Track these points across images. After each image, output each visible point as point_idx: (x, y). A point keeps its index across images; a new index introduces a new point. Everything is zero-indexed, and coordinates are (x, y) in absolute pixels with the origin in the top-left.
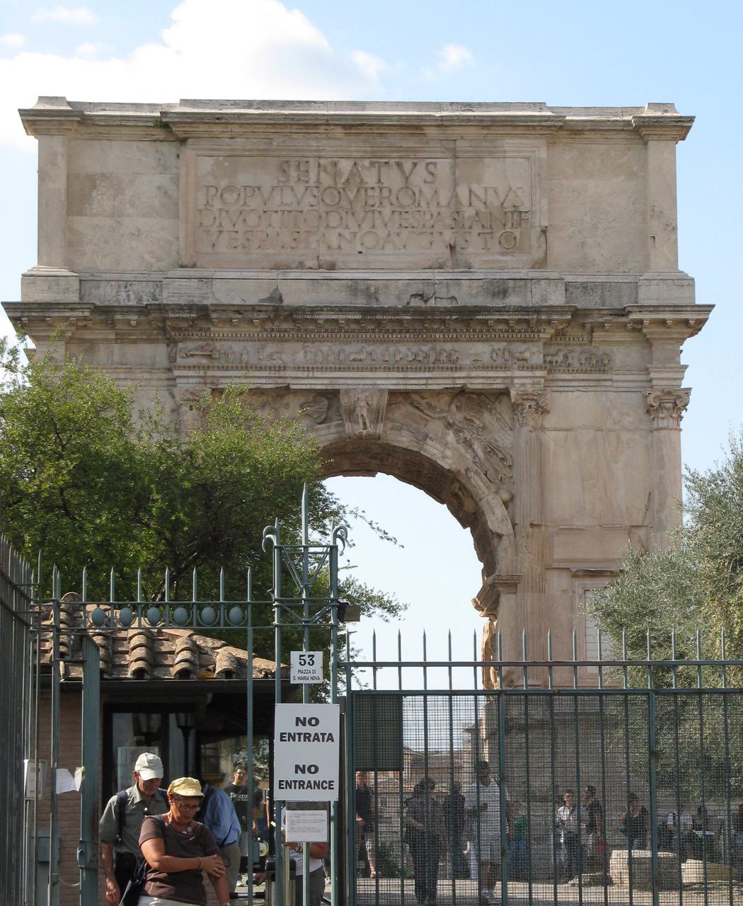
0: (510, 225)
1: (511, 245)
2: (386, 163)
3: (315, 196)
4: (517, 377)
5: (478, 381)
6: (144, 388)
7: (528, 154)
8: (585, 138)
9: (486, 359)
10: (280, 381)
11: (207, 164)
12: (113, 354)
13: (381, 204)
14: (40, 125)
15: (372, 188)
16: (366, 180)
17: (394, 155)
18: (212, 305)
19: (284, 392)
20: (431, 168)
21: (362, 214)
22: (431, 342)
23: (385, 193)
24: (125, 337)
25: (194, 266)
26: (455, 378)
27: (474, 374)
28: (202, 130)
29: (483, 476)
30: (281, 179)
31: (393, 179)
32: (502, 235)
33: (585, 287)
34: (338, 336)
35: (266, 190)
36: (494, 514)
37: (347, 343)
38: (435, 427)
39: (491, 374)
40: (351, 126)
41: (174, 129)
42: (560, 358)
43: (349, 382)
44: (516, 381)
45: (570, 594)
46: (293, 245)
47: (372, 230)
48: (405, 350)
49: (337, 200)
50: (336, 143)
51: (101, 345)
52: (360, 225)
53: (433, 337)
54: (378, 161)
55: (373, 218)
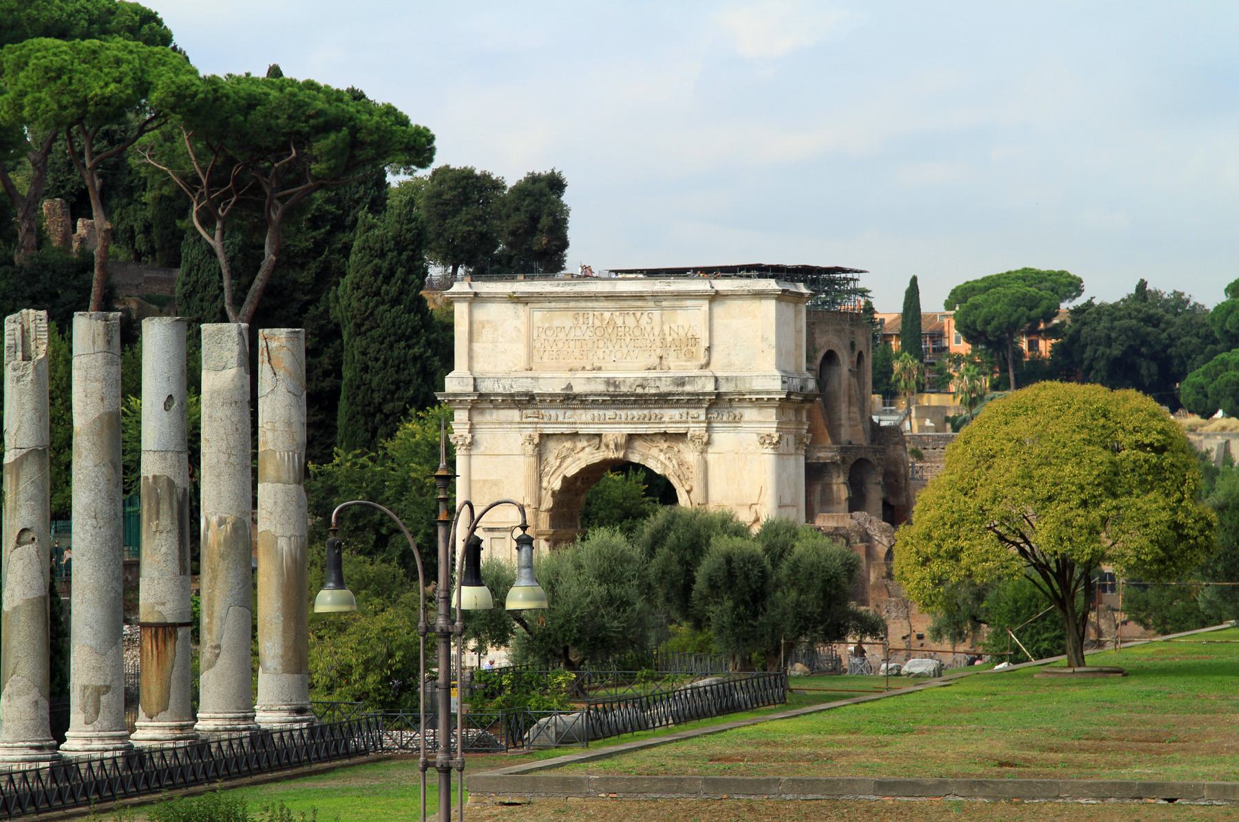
1: (691, 356)
9: (677, 418)
19: (575, 435)
23: (627, 329)
31: (630, 321)
35: (567, 329)
37: (606, 409)
38: (654, 451)
39: (678, 425)
48: (636, 413)
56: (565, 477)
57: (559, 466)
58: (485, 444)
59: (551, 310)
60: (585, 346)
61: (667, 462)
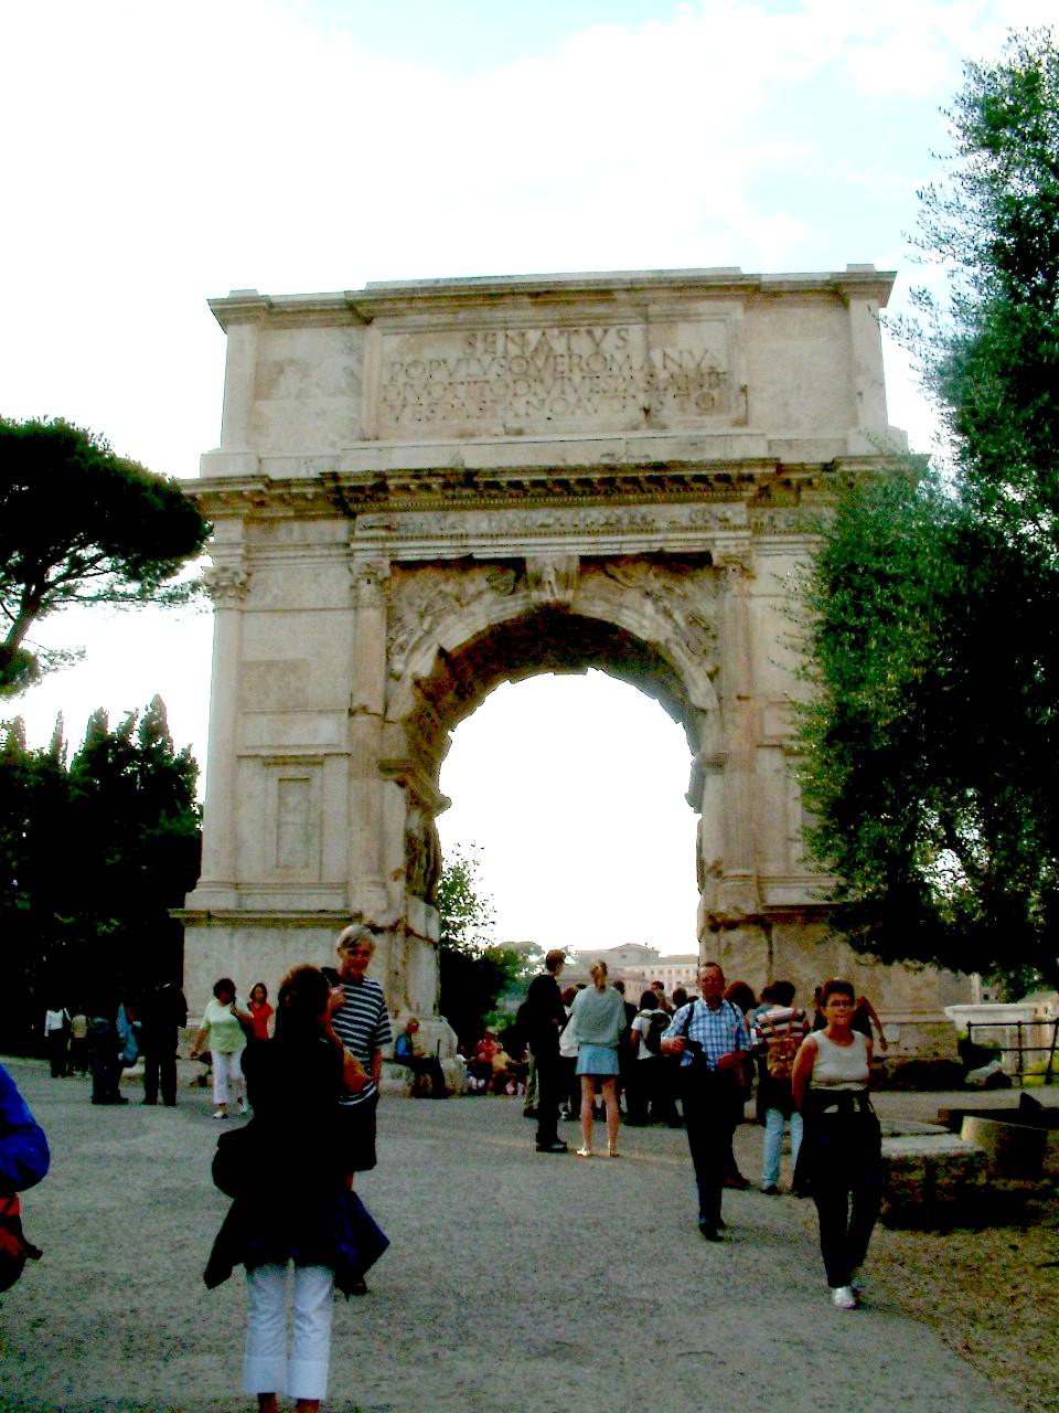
0: (707, 385)
1: (708, 405)
2: (576, 331)
5: (676, 544)
9: (685, 522)
10: (462, 550)
11: (392, 343)
13: (571, 370)
15: (562, 356)
16: (556, 348)
19: (467, 564)
20: (623, 333)
23: (575, 360)
25: (377, 439)
26: (649, 541)
27: (671, 536)
29: (686, 648)
31: (582, 344)
32: (699, 396)
33: (789, 444)
35: (452, 362)
37: (533, 507)
39: (691, 535)
40: (537, 295)
42: (766, 520)
43: (538, 548)
48: (597, 514)
49: (524, 369)
50: (527, 311)
52: (548, 393)
56: (442, 652)
57: (428, 633)
58: (275, 591)
59: (418, 331)
60: (487, 392)
61: (661, 619)
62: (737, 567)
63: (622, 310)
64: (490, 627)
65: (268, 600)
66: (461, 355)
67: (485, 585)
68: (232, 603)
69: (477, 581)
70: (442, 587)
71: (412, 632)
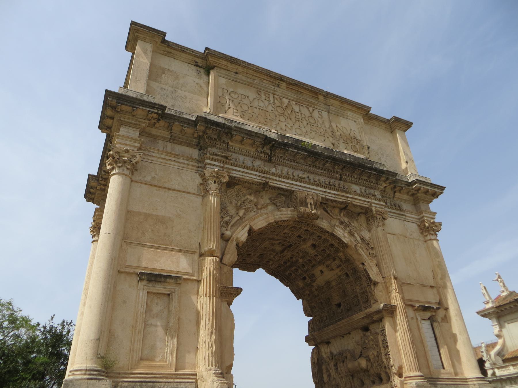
2: (302, 105)
3: (273, 107)
4: (374, 203)
6: (184, 169)
7: (356, 120)
8: (372, 123)
10: (264, 179)
12: (166, 147)
14: (141, 34)
17: (305, 103)
18: (234, 126)
19: (265, 185)
20: (320, 113)
21: (295, 121)
22: (334, 179)
23: (303, 116)
24: (176, 139)
28: (223, 64)
30: (258, 96)
32: (352, 145)
34: (293, 164)
35: (251, 98)
36: (372, 270)
40: (290, 84)
41: (210, 59)
44: (373, 205)
45: (415, 320)
46: (265, 123)
47: (299, 128)
49: (283, 112)
51: (160, 141)
52: (294, 125)
53: (336, 175)
54: (298, 103)
55: (299, 123)
62: (381, 217)
63: (320, 103)
64: (276, 222)
65: (148, 178)
66: (255, 97)
67: (268, 201)
68: (127, 172)
69: (265, 199)
70: (248, 197)
71: (232, 217)
